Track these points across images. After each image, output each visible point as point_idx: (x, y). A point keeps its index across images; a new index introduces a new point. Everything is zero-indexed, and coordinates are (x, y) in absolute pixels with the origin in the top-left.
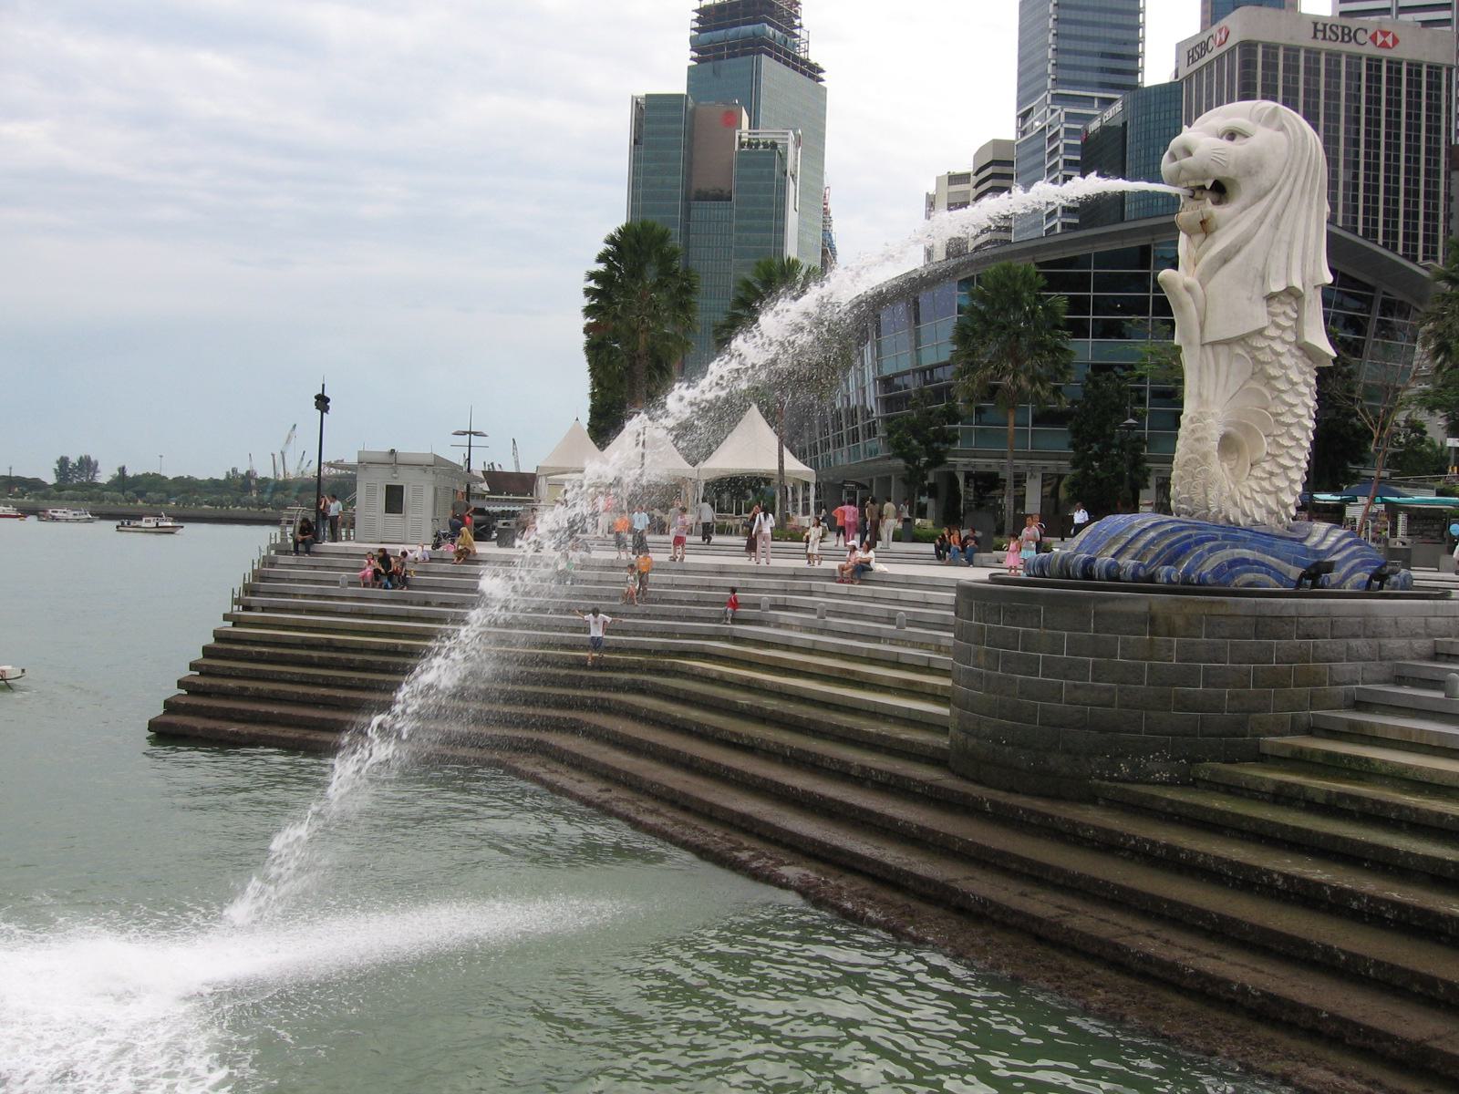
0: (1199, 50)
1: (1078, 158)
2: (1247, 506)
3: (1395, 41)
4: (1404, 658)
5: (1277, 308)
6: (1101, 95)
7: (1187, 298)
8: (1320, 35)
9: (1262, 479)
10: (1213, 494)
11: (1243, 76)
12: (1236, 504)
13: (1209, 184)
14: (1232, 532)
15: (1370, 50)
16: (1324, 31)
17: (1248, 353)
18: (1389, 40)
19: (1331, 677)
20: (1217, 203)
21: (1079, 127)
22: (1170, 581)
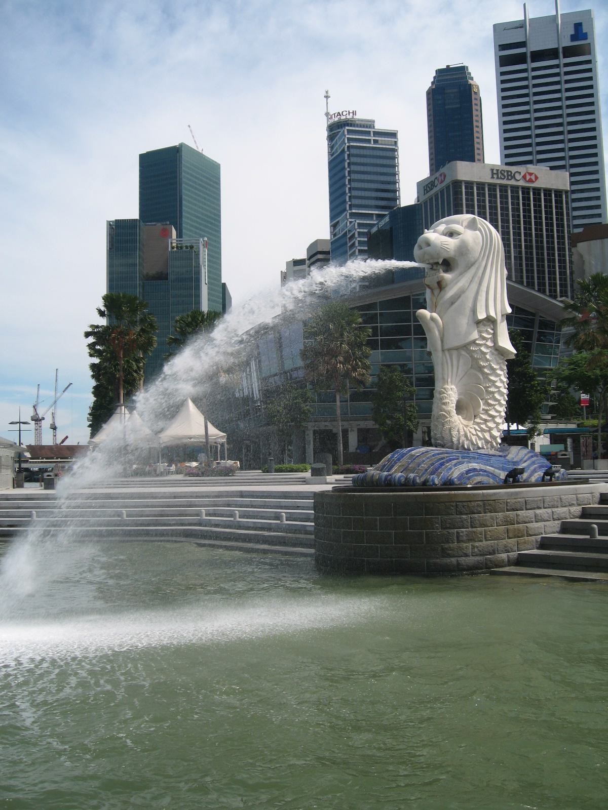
0: (430, 186)
1: (366, 248)
2: (474, 438)
4: (567, 519)
5: (482, 328)
6: (377, 212)
7: (432, 325)
8: (495, 176)
9: (480, 423)
10: (454, 433)
11: (455, 199)
12: (467, 439)
13: (441, 261)
15: (522, 183)
16: (497, 174)
17: (468, 354)
19: (527, 531)
20: (446, 271)
21: (366, 231)
22: (434, 484)
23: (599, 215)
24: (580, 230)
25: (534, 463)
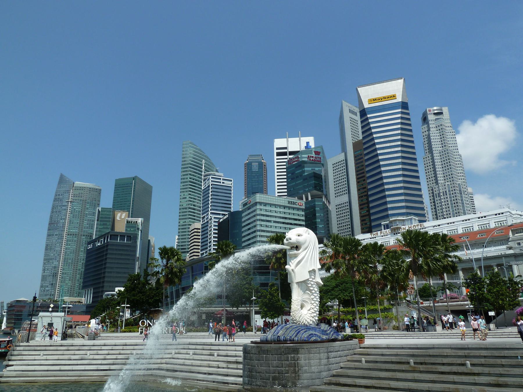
14: (307, 327)
25: (331, 331)
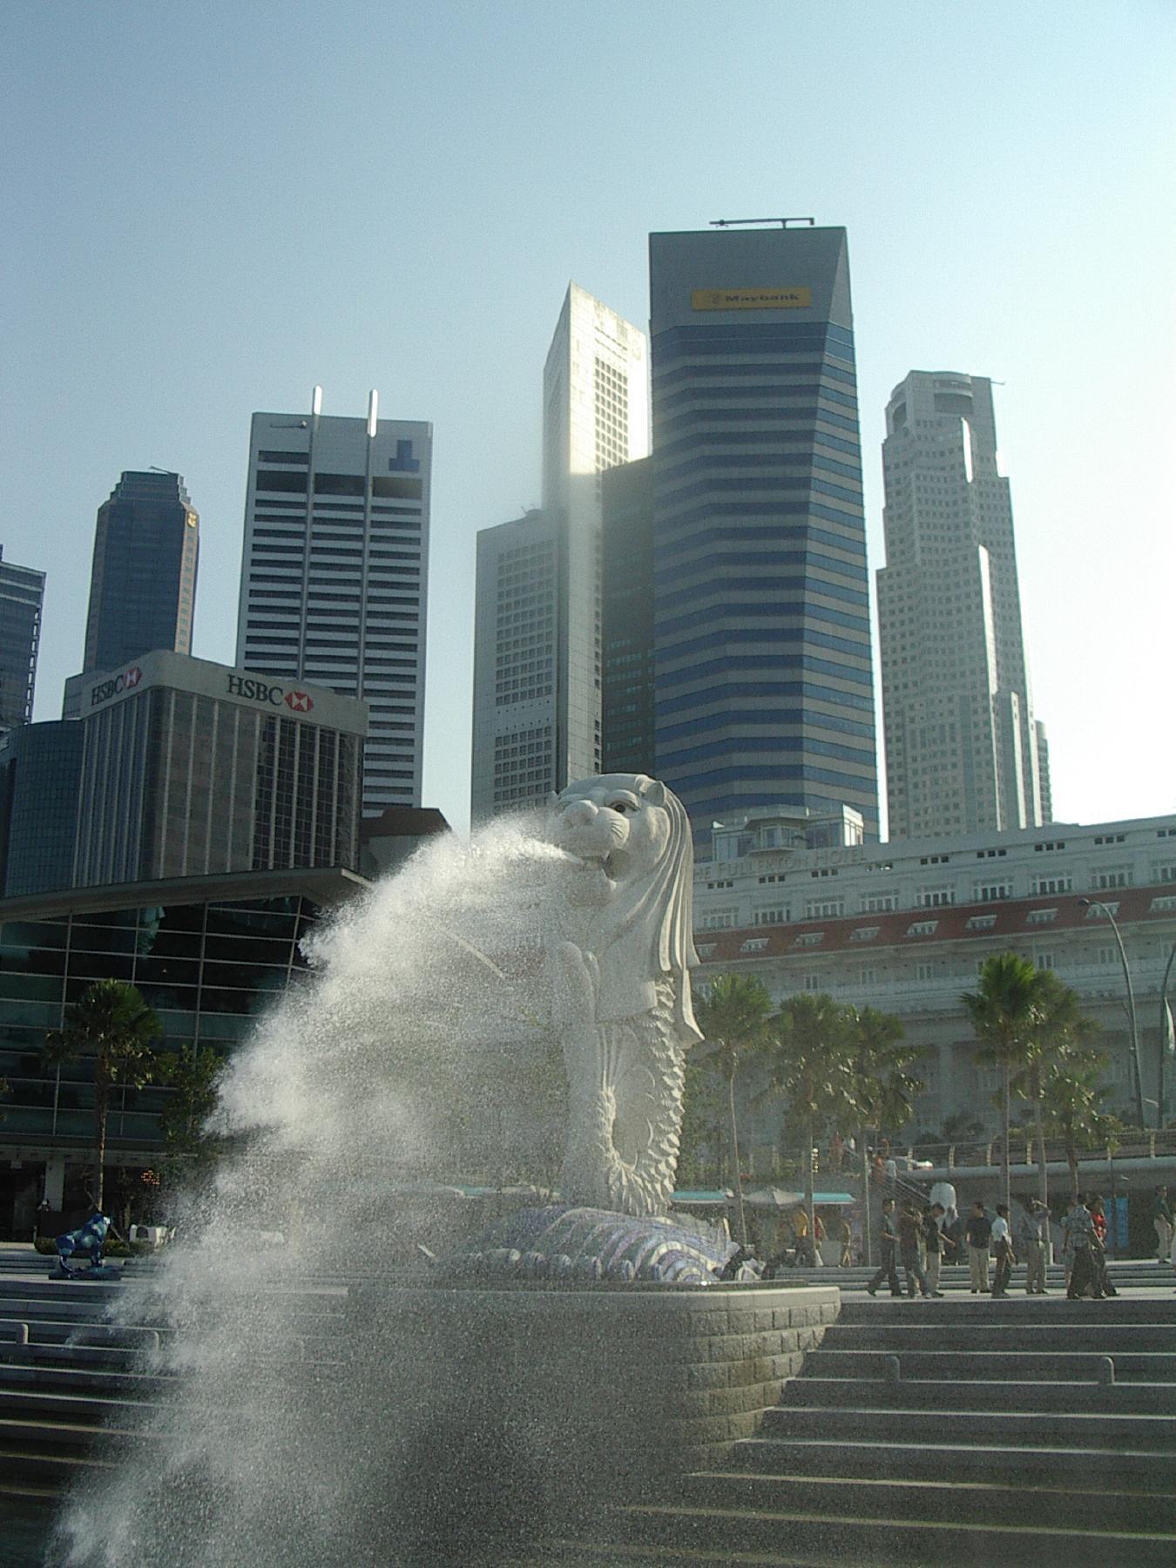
3: (310, 704)
8: (235, 689)
15: (284, 711)
18: (304, 702)
23: (409, 790)
24: (379, 813)
